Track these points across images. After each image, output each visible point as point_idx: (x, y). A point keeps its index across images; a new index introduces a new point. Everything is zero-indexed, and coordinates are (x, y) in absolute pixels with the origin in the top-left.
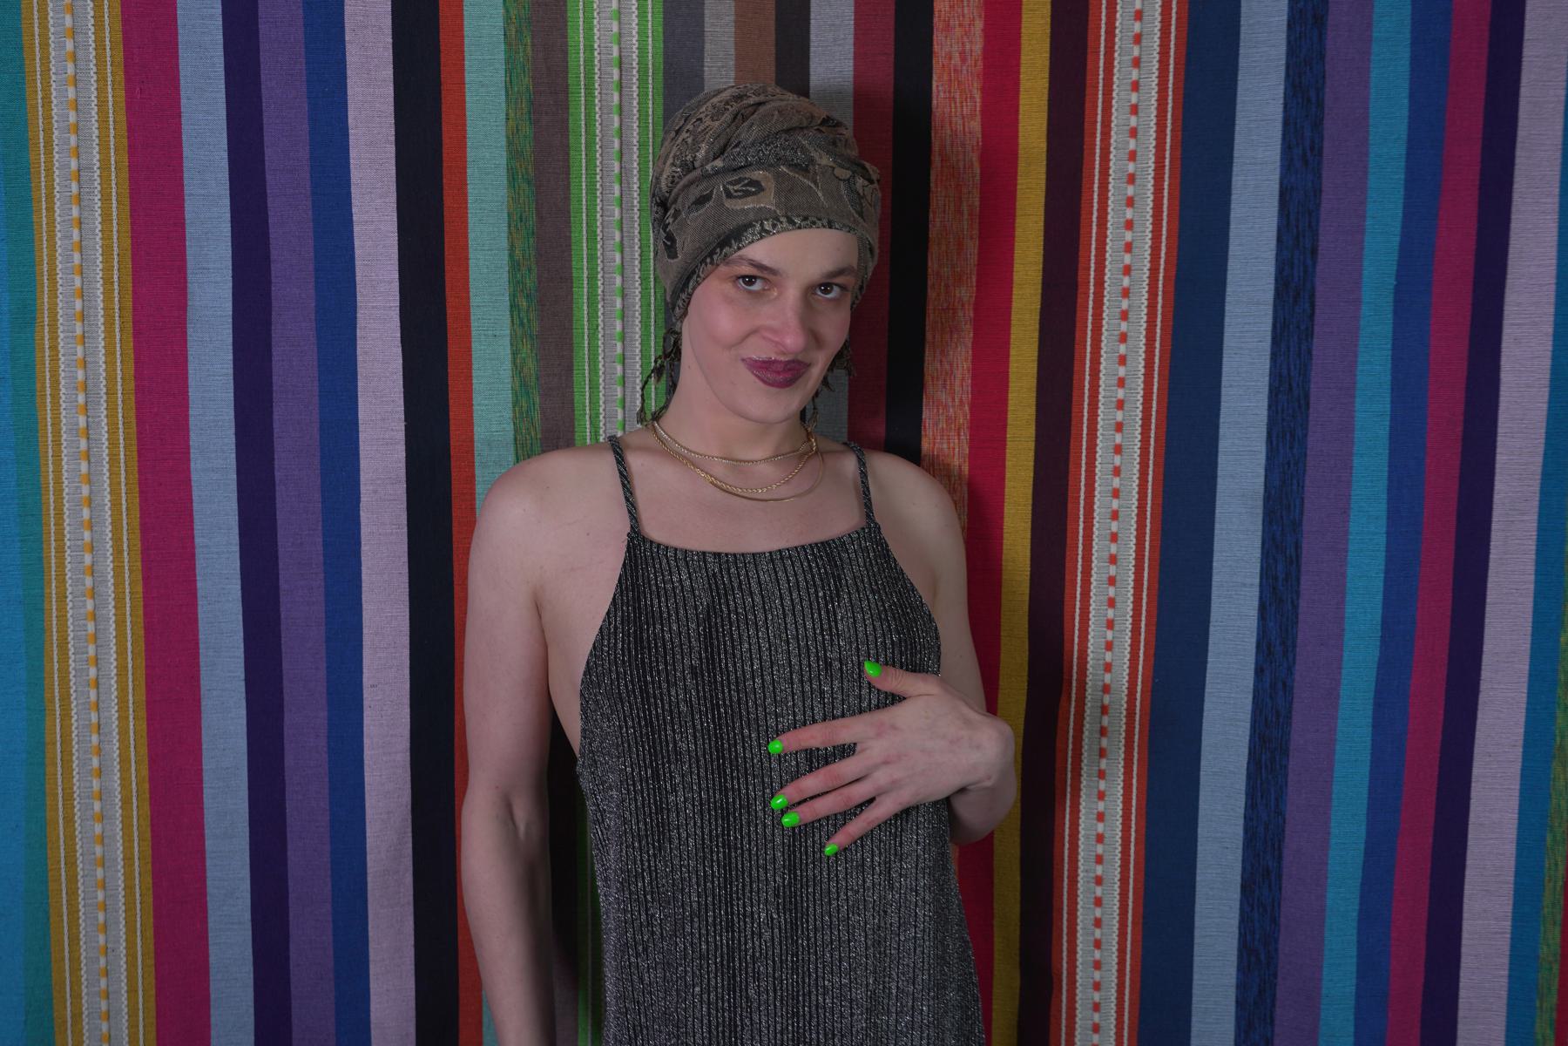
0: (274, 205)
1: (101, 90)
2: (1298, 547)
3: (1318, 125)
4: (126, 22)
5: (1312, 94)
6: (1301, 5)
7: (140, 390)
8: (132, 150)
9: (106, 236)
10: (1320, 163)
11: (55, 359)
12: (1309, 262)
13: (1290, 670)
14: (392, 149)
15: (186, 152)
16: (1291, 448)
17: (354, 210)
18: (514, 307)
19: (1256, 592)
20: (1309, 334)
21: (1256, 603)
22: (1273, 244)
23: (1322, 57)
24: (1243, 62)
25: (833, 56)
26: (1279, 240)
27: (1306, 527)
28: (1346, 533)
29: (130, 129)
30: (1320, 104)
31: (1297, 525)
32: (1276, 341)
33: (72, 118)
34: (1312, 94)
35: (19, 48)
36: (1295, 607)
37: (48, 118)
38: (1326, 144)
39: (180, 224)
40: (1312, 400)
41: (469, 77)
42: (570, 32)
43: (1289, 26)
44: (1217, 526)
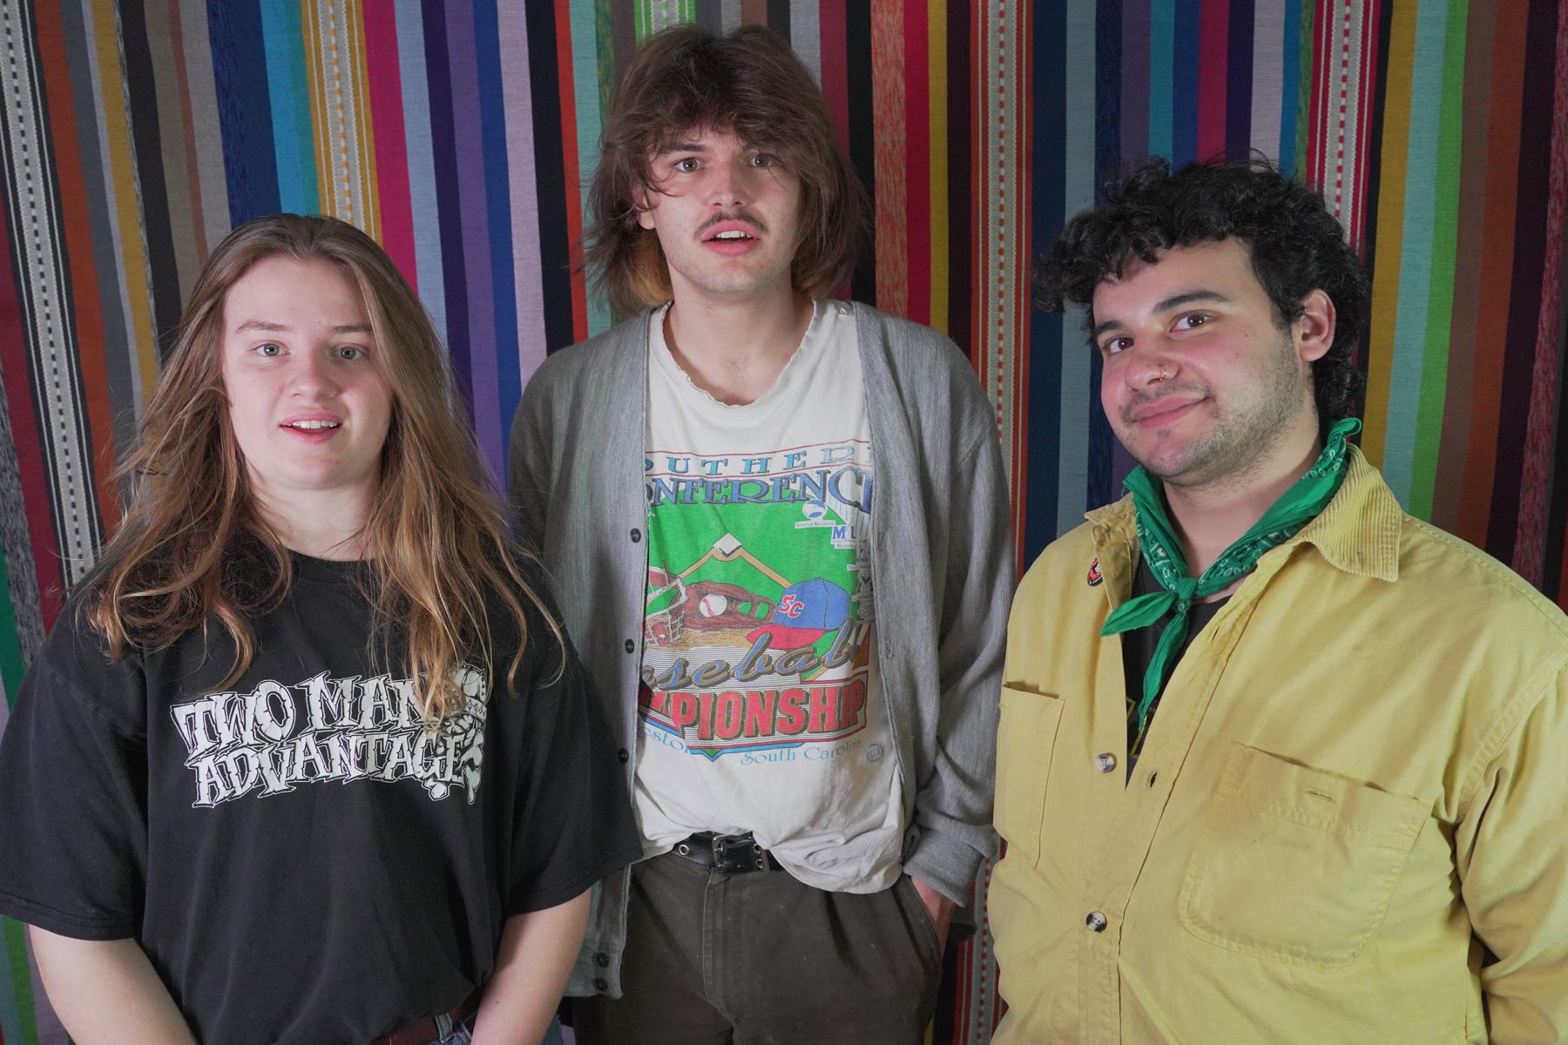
0: (468, 250)
4: (377, 143)
14: (535, 214)
15: (415, 219)
24: (1068, 148)
35: (314, 160)
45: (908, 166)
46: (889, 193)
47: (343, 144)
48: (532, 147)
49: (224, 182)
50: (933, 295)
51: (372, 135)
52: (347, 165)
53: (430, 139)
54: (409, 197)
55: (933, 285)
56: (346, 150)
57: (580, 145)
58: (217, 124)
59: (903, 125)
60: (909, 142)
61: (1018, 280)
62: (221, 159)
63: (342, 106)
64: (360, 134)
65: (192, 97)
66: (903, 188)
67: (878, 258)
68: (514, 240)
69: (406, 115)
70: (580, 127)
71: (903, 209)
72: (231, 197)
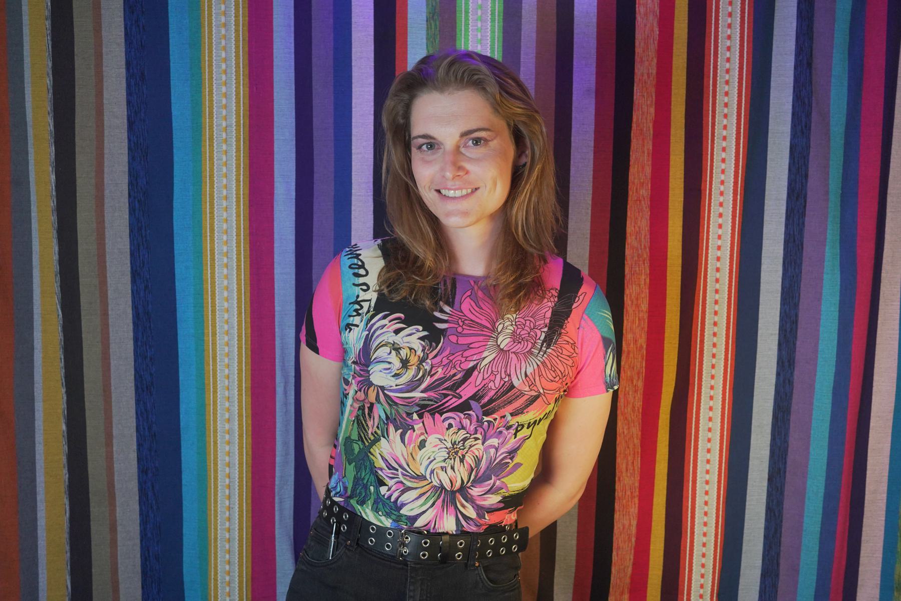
1: (237, 88)
2: (797, 316)
3: (809, 116)
6: (801, 58)
7: (251, 234)
8: (251, 116)
9: (238, 159)
10: (809, 133)
11: (212, 218)
13: (792, 374)
15: (276, 119)
17: (353, 148)
19: (777, 337)
20: (803, 215)
21: (777, 343)
22: (787, 172)
23: (811, 83)
24: (773, 84)
26: (790, 170)
28: (820, 311)
29: (251, 106)
30: (810, 105)
31: (796, 306)
33: (224, 102)
35: (200, 68)
36: (795, 344)
37: (211, 101)
38: (813, 125)
39: (272, 153)
40: (805, 246)
44: (761, 307)
46: (643, 114)
47: (223, 55)
48: (373, 64)
49: (124, 81)
50: (671, 193)
51: (247, 49)
52: (225, 72)
54: (272, 101)
55: (671, 185)
56: (225, 60)
58: (123, 34)
59: (655, 61)
61: (736, 183)
62: (123, 63)
63: (225, 25)
64: (237, 47)
65: (103, 12)
67: (631, 163)
68: (354, 139)
69: (275, 35)
72: (129, 93)
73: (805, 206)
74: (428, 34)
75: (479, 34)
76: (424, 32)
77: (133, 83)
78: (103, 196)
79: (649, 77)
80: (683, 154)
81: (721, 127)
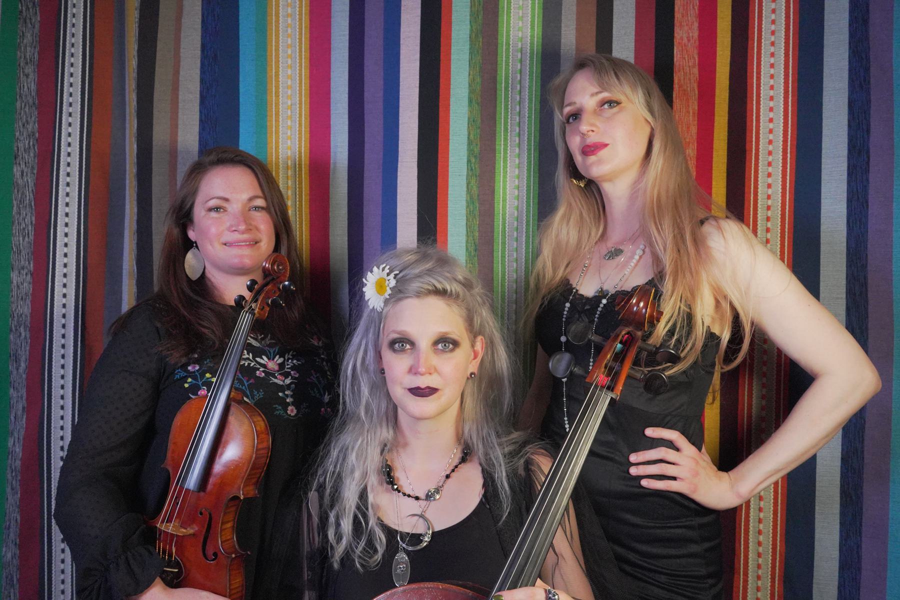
5: (864, 57)
12: (866, 136)
14: (418, 90)
16: (860, 228)
18: (469, 161)
20: (867, 171)
22: (846, 128)
23: (867, 38)
25: (624, 46)
26: (850, 126)
27: (869, 268)
31: (864, 267)
32: (850, 174)
34: (864, 57)
35: (265, 50)
38: (872, 81)
41: (453, 57)
42: (499, 37)
43: (850, 25)
45: (699, 54)
46: (685, 74)
50: (715, 154)
53: (347, 38)
57: (453, 41)
59: (696, 25)
60: (700, 36)
66: (696, 71)
70: (455, 27)
71: (696, 86)
73: (868, 163)
74: (471, 11)
75: (521, 12)
76: (468, 10)
77: (206, 63)
78: (176, 161)
79: (689, 40)
80: (727, 115)
81: (768, 87)
